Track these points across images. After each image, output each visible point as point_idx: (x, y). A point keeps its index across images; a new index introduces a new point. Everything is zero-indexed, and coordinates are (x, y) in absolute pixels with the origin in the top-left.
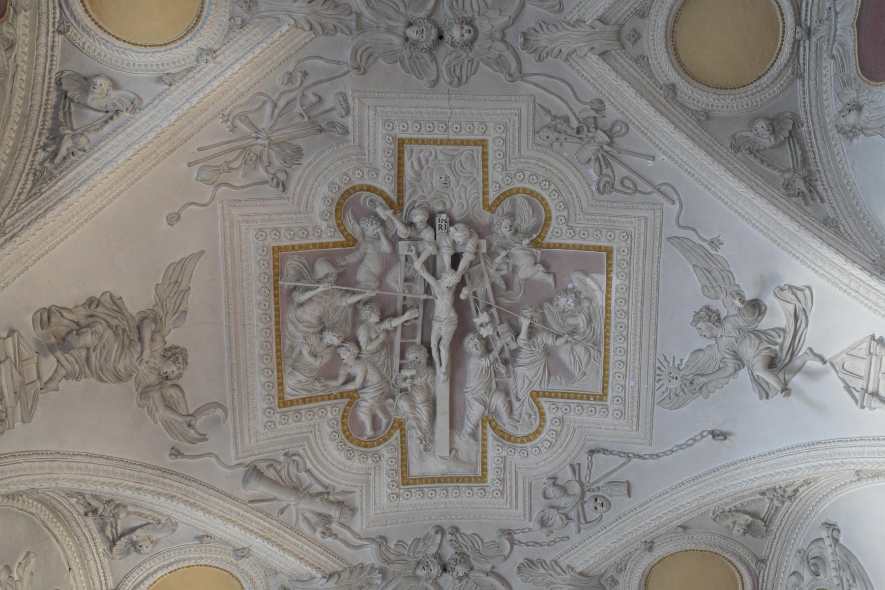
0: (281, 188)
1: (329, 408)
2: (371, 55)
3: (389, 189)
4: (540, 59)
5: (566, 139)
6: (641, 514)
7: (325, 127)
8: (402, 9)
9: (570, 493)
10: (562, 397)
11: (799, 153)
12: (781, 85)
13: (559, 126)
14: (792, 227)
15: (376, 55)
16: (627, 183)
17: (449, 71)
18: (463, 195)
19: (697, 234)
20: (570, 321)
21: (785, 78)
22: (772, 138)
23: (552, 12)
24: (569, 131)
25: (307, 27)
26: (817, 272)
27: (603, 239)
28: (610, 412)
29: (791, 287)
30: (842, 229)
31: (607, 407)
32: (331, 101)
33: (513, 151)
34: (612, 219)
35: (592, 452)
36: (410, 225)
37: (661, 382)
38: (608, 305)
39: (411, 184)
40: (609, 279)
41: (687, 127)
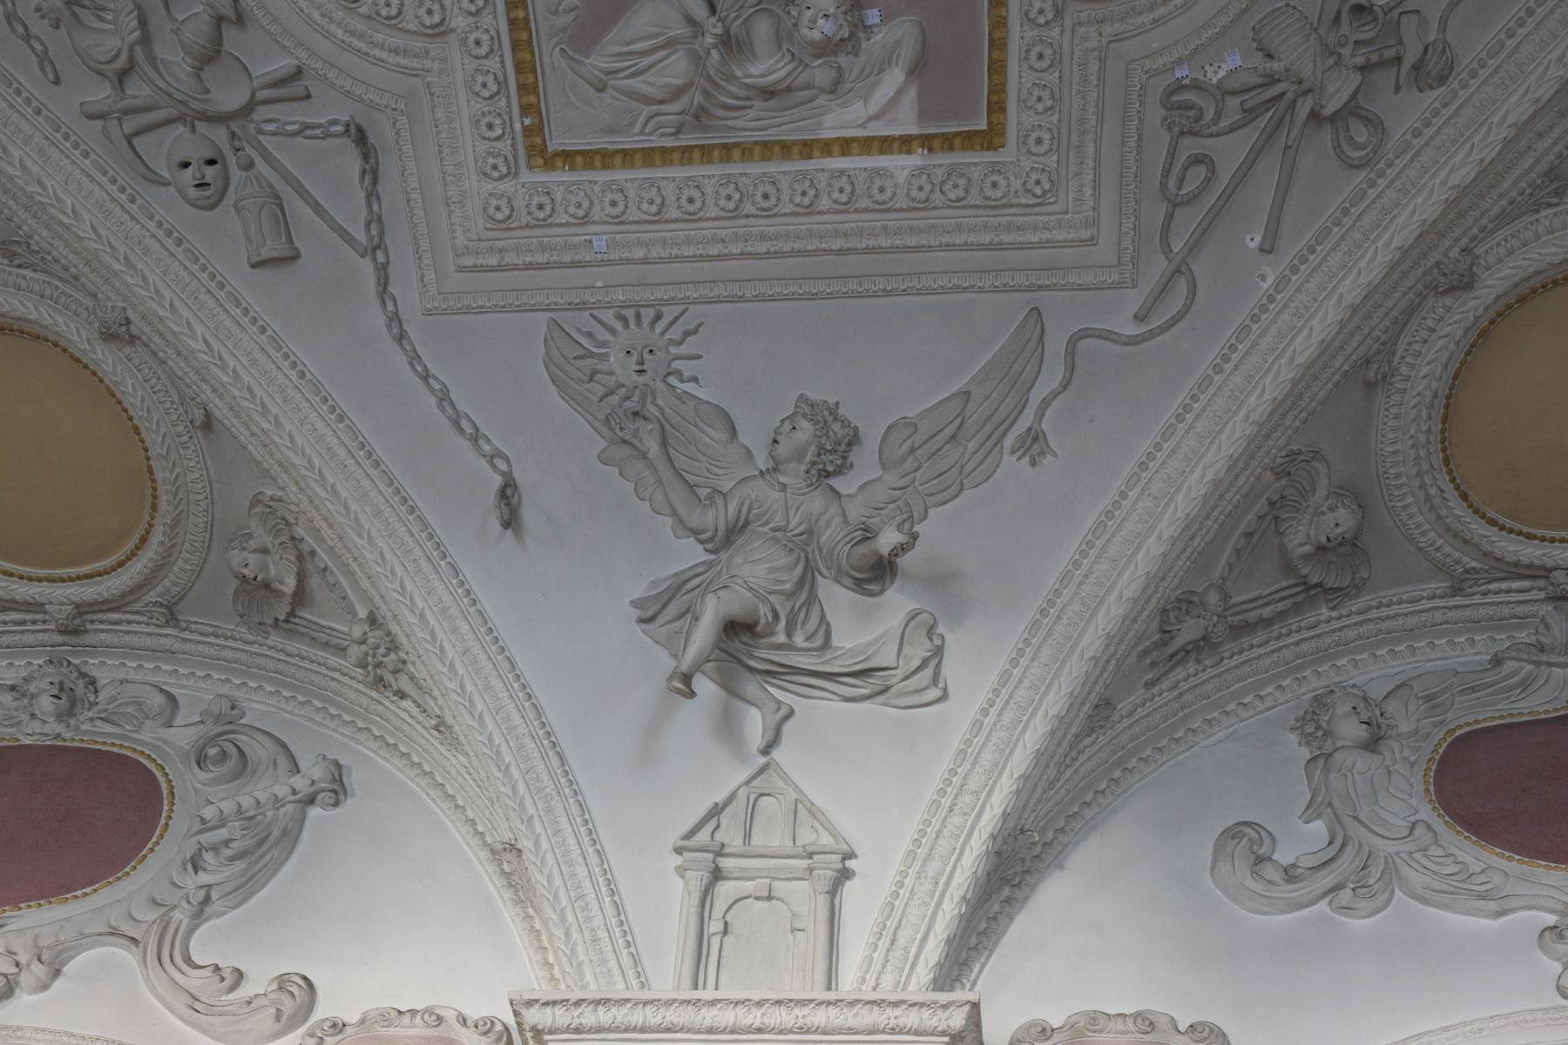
6: (211, 303)
9: (207, 73)
10: (513, 23)
11: (1266, 612)
12: (1438, 549)
14: (1092, 641)
19: (1055, 395)
20: (762, 30)
21: (1457, 554)
22: (1308, 548)
26: (985, 712)
27: (1030, 119)
28: (504, 186)
29: (939, 651)
30: (1088, 741)
31: (513, 173)
35: (360, 137)
37: (619, 326)
38: (828, 147)
40: (905, 144)
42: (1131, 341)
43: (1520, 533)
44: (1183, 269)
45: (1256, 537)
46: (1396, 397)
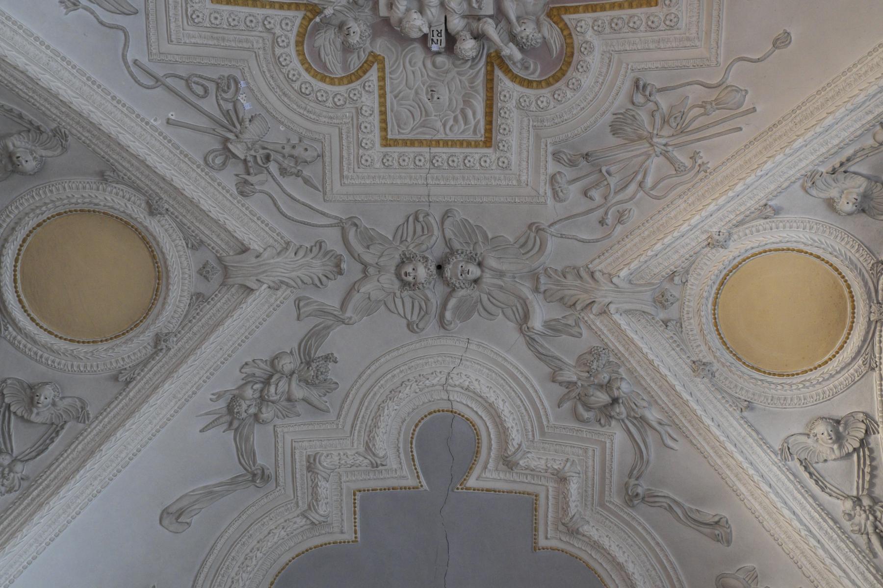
0: (641, 83)
2: (522, 246)
3: (504, 83)
4: (320, 244)
5: (283, 148)
7: (582, 160)
8: (485, 297)
12: (8, 216)
13: (292, 164)
15: (517, 246)
16: (200, 90)
17: (430, 229)
18: (411, 76)
22: (11, 147)
23: (309, 298)
24: (280, 158)
25: (598, 275)
32: (573, 191)
33: (348, 132)
34: (216, 42)
36: (478, 36)
39: (476, 91)
41: (129, 162)
42: (124, 57)
43: (18, 254)
44: (159, 83)
45: (19, 121)
46: (94, 186)
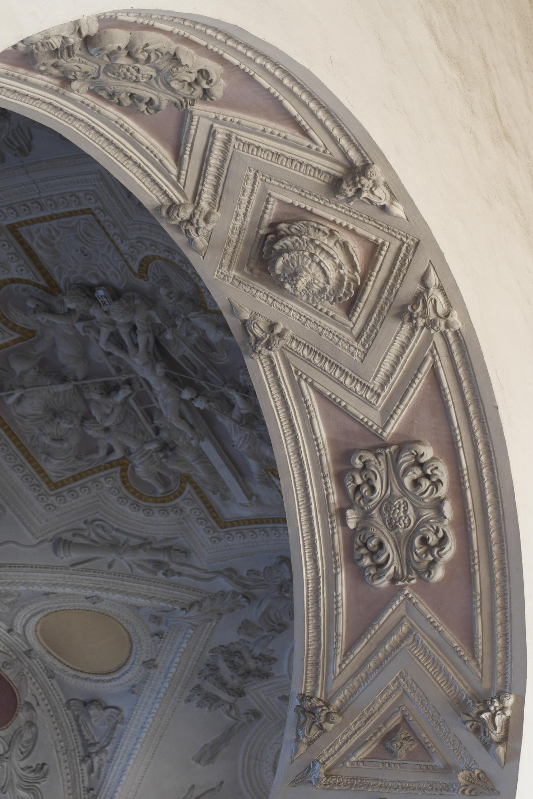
1: (102, 480)
